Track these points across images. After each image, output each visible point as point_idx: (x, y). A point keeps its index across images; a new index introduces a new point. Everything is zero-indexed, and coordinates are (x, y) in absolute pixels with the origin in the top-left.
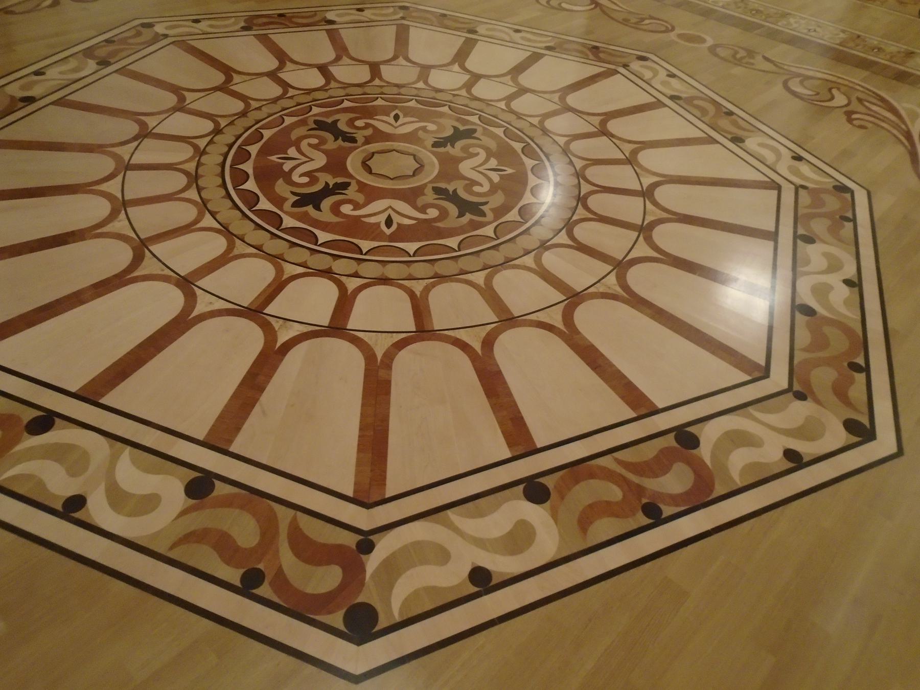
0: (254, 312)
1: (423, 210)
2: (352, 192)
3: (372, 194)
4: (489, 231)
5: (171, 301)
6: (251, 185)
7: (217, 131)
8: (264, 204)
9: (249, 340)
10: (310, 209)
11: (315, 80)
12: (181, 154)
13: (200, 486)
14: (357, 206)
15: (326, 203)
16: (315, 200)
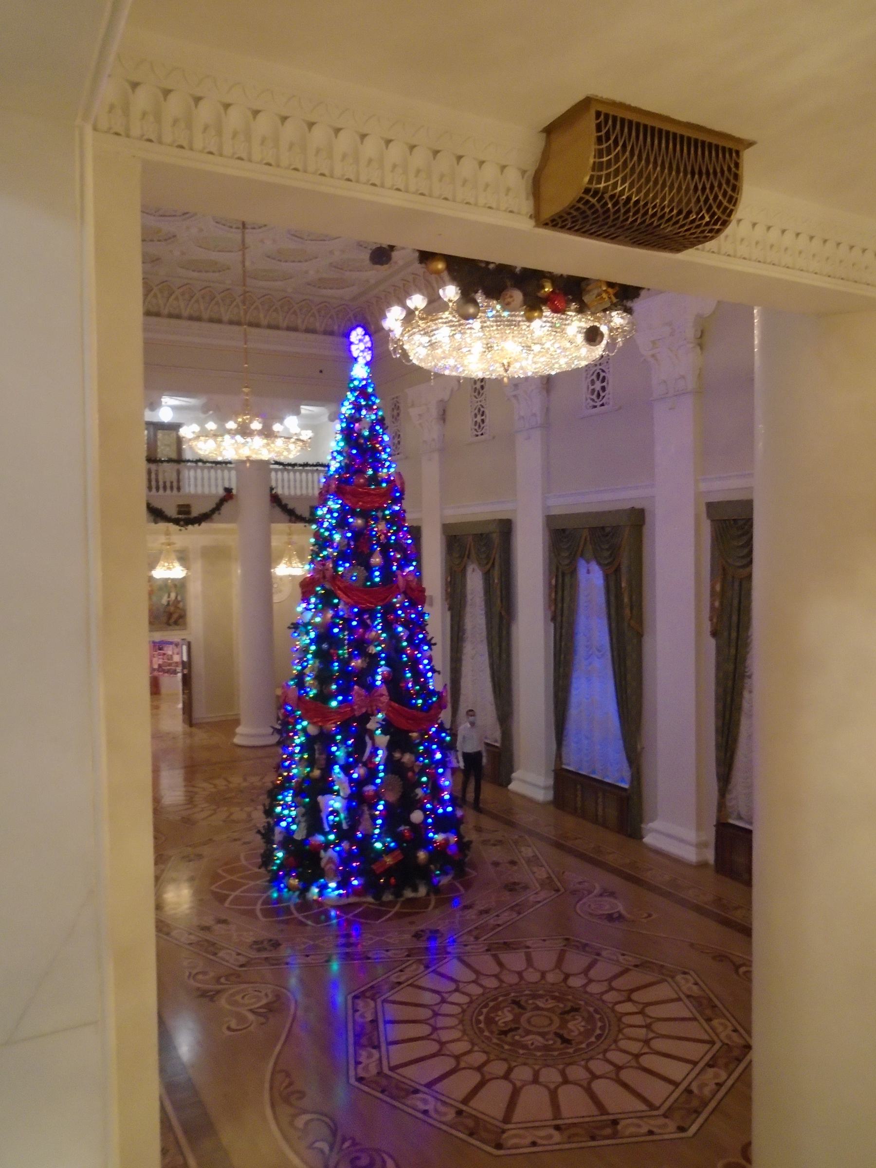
0: (479, 1069)
1: (547, 1040)
2: (520, 1031)
3: (528, 1033)
4: (571, 1051)
5: (450, 1063)
6: (482, 1025)
7: (471, 1002)
8: (487, 1033)
9: (476, 1078)
10: (503, 1036)
11: (515, 979)
12: (456, 1010)
13: (460, 1113)
14: (522, 1037)
15: (510, 1035)
16: (505, 1033)
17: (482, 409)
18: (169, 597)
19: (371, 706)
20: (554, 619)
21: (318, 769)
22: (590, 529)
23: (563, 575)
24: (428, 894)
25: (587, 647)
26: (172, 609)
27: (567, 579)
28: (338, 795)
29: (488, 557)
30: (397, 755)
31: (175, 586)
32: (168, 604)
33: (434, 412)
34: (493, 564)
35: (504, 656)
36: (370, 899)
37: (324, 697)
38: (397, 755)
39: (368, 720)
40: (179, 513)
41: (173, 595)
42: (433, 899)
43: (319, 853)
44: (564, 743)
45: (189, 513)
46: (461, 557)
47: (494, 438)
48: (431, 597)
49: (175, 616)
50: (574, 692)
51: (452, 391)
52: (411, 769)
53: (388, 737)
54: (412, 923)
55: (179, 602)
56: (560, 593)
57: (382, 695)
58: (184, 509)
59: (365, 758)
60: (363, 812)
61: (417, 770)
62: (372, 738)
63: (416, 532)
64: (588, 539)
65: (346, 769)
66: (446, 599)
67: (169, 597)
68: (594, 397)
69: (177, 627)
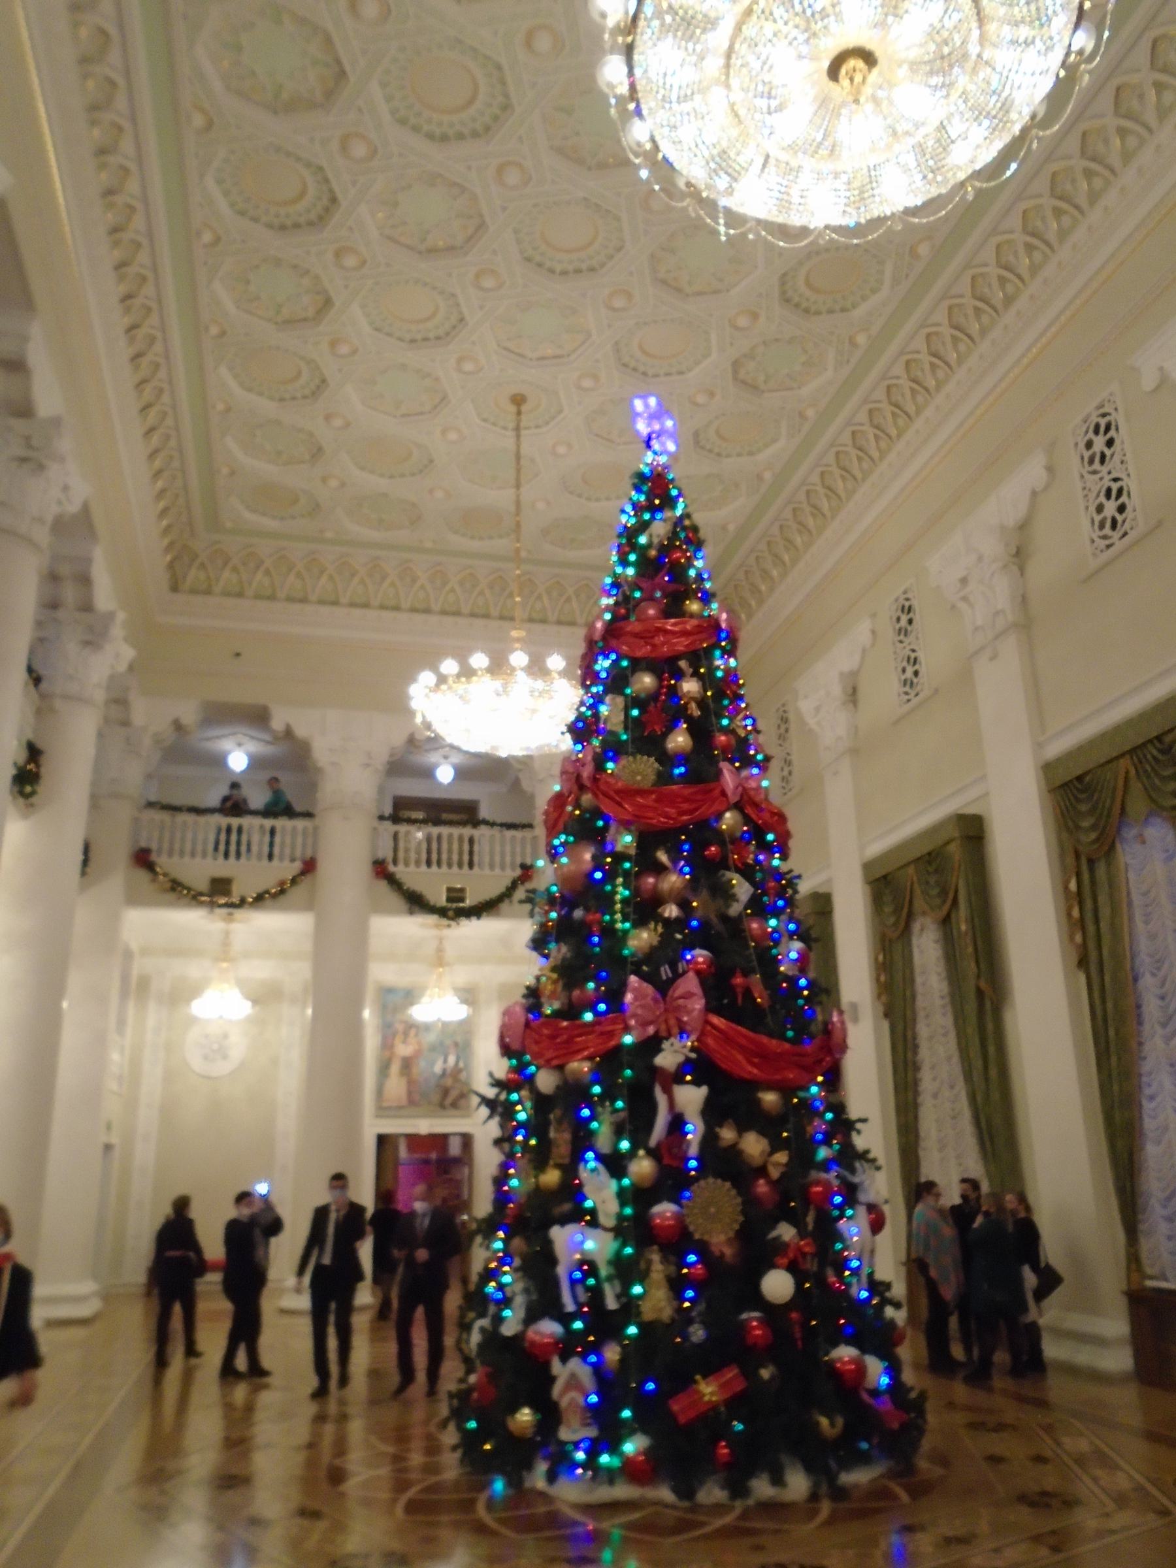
17: (913, 655)
18: (445, 1061)
19: (666, 1021)
20: (1083, 963)
21: (558, 1166)
22: (1132, 751)
23: (1091, 862)
24: (814, 1497)
25: (1162, 998)
26: (449, 1082)
27: (1101, 871)
28: (594, 1223)
29: (944, 893)
30: (727, 1134)
31: (456, 1044)
32: (444, 1074)
33: (837, 690)
34: (955, 901)
35: (993, 1072)
36: (665, 1493)
37: (571, 1012)
38: (727, 1134)
39: (658, 1050)
40: (449, 900)
41: (452, 1060)
42: (826, 1508)
43: (547, 1365)
44: (1142, 1227)
45: (462, 900)
46: (897, 911)
47: (936, 691)
48: (854, 1007)
49: (453, 1094)
50: (1147, 1106)
51: (864, 651)
52: (762, 1171)
53: (703, 1091)
54: (759, 1548)
55: (460, 1071)
56: (1089, 905)
57: (688, 996)
58: (456, 895)
59: (653, 1141)
60: (649, 1263)
61: (775, 1173)
62: (668, 1091)
63: (823, 903)
64: (1133, 772)
65: (615, 1164)
66: (879, 996)
67: (445, 1061)
68: (1107, 530)
69: (453, 1112)
